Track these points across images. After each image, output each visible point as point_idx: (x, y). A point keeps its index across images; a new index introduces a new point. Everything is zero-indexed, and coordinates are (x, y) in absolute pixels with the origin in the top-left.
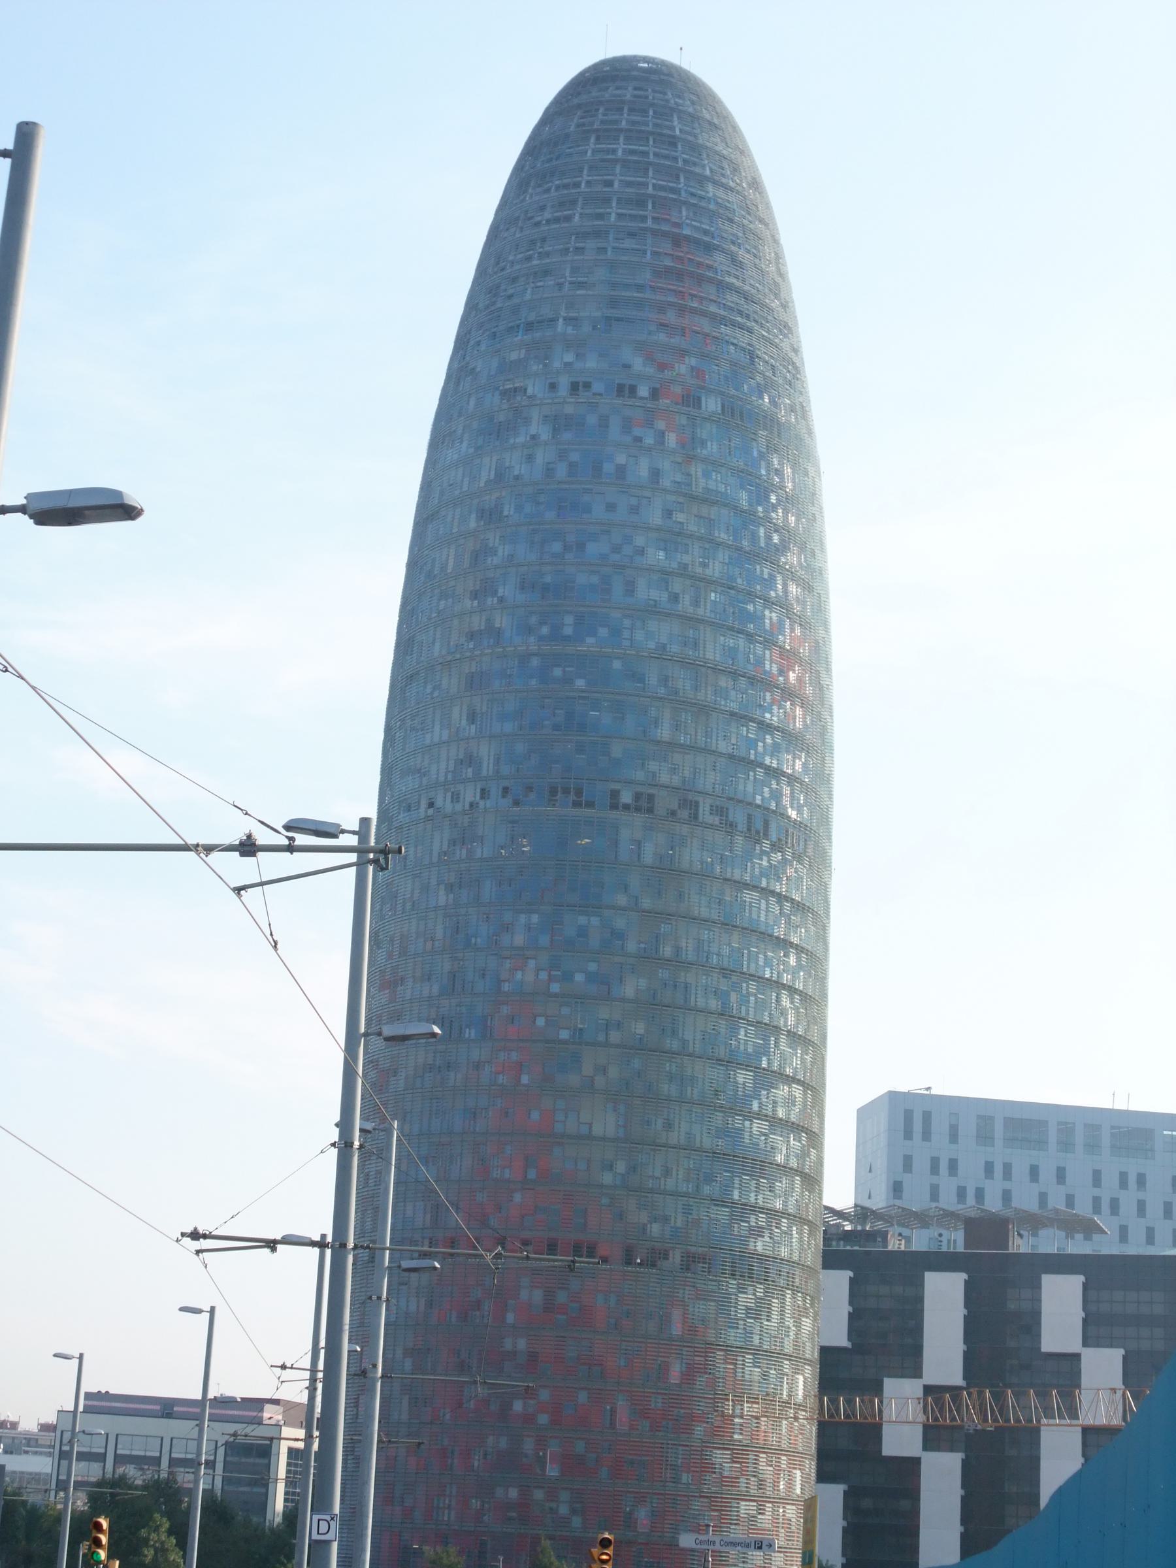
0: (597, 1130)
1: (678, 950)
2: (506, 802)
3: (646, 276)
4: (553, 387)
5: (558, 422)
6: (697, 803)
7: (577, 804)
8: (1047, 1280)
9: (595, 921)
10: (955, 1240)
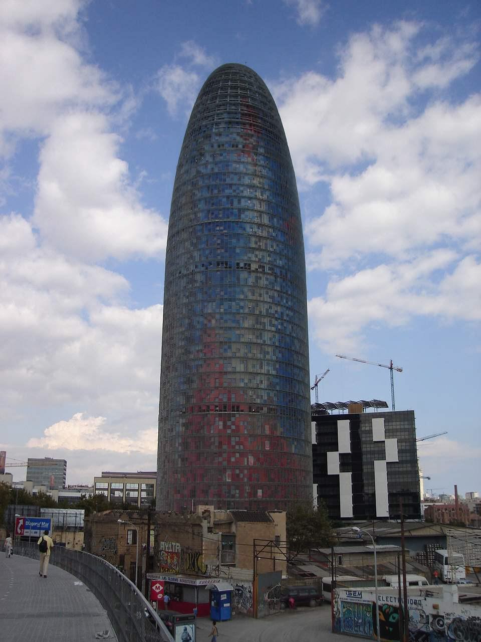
0: (238, 369)
1: (261, 312)
2: (203, 269)
3: (239, 116)
4: (212, 146)
5: (213, 156)
6: (264, 267)
7: (227, 268)
8: (374, 420)
9: (234, 303)
10: (346, 412)
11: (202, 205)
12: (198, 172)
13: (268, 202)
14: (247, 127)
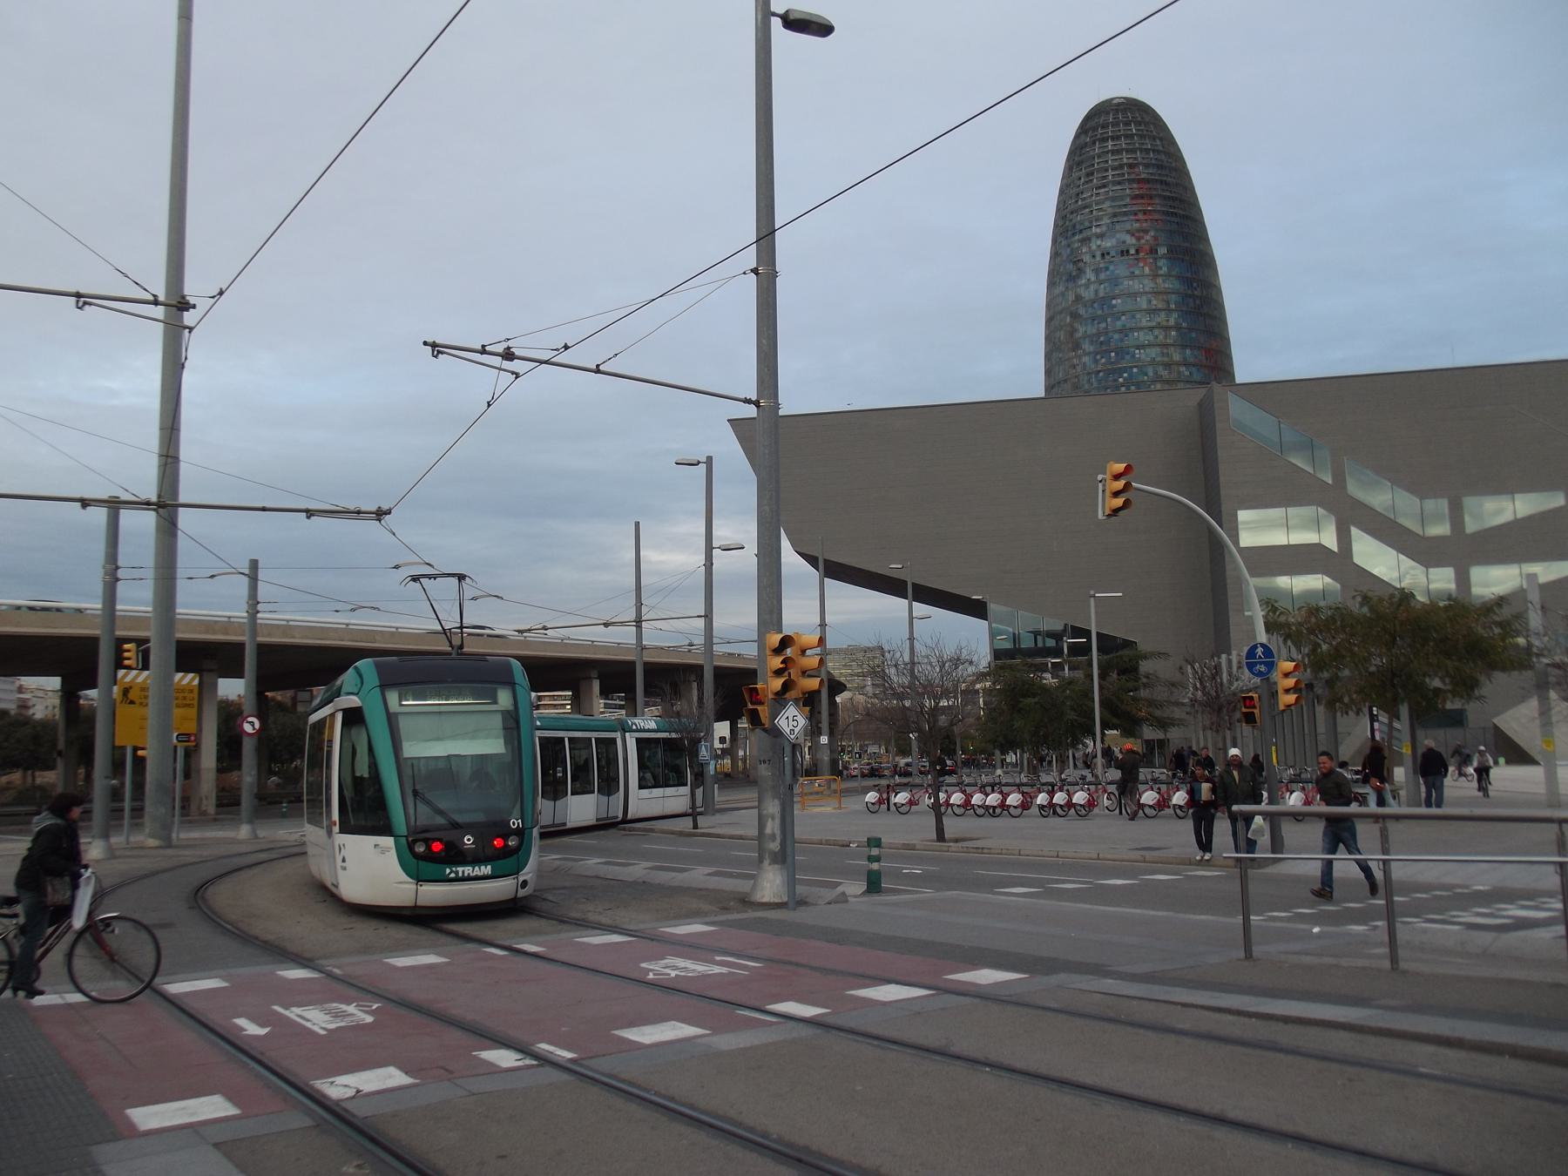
3: (1128, 200)
5: (1097, 271)
11: (1087, 346)
12: (1078, 298)
13: (1178, 328)
14: (1141, 216)
